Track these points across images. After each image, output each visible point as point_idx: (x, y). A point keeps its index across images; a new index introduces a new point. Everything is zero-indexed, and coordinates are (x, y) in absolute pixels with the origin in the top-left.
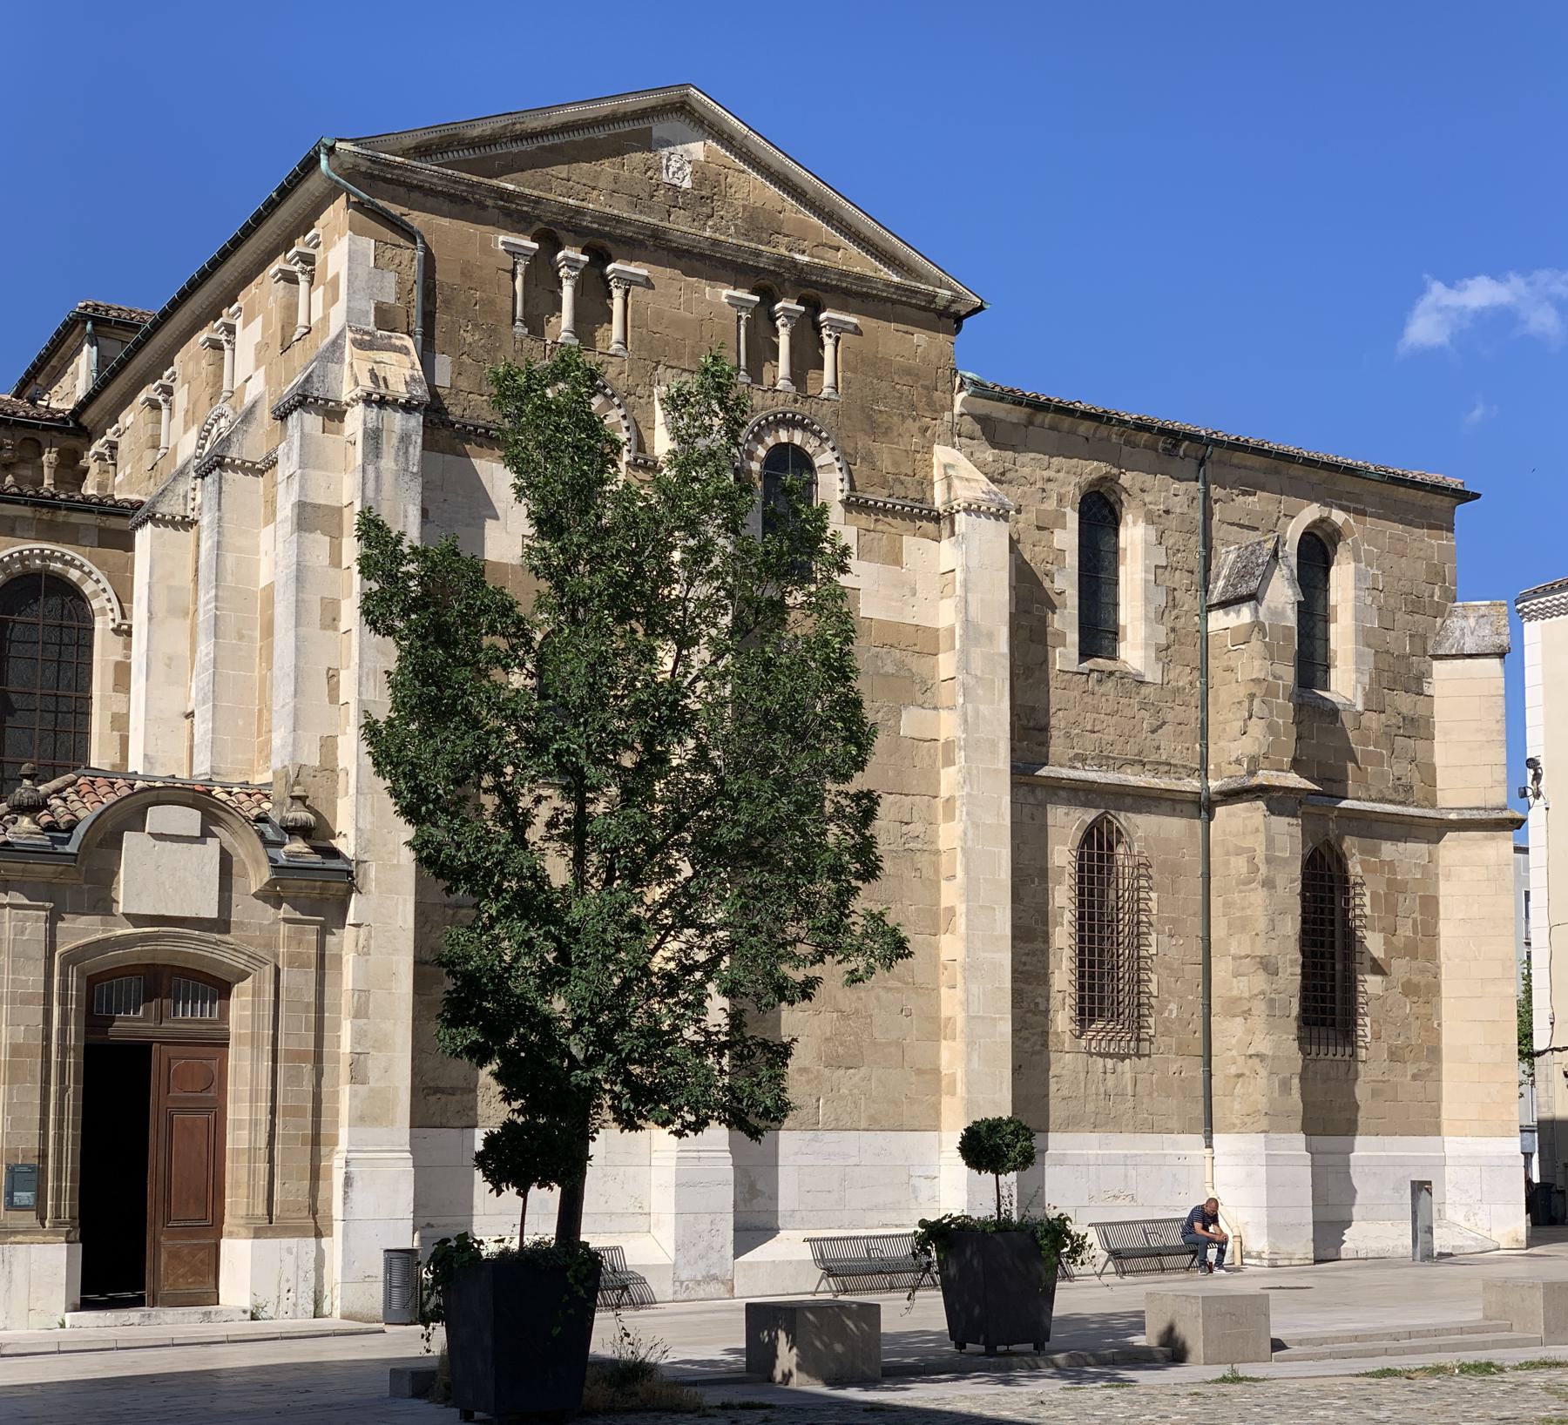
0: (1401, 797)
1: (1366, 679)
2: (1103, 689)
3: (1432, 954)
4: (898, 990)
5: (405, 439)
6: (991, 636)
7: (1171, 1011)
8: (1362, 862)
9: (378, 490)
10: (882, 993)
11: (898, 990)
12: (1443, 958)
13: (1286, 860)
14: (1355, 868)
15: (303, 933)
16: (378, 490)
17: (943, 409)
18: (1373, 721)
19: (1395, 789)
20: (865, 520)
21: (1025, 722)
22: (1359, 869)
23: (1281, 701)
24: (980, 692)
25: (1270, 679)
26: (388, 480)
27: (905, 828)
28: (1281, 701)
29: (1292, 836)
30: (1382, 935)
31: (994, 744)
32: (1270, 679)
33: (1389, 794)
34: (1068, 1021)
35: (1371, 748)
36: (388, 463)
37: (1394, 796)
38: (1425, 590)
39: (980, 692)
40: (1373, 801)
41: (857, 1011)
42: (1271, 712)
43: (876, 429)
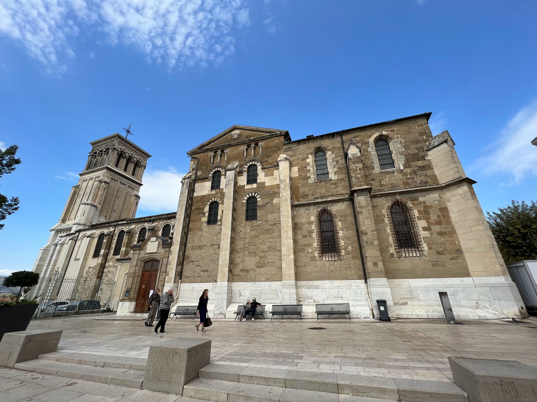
0: (424, 185)
1: (403, 162)
2: (321, 184)
3: (449, 222)
4: (273, 251)
5: (187, 182)
6: (285, 181)
7: (349, 249)
8: (412, 204)
9: (183, 190)
10: (270, 252)
11: (273, 251)
12: (454, 223)
13: (366, 206)
14: (410, 204)
15: (166, 253)
16: (183, 190)
17: (281, 149)
18: (408, 170)
19: (421, 183)
20: (266, 170)
21: (302, 195)
22: (411, 205)
23: (359, 171)
24: (283, 191)
25: (354, 168)
26: (184, 188)
27: (276, 220)
28: (359, 171)
29: (366, 200)
30: (425, 220)
31: (287, 200)
32: (354, 168)
33: (418, 185)
34: (317, 254)
35: (409, 176)
36: (185, 186)
37: (421, 185)
38: (421, 138)
39: (283, 191)
40: (412, 188)
41: (264, 256)
42: (356, 175)
43: (268, 157)
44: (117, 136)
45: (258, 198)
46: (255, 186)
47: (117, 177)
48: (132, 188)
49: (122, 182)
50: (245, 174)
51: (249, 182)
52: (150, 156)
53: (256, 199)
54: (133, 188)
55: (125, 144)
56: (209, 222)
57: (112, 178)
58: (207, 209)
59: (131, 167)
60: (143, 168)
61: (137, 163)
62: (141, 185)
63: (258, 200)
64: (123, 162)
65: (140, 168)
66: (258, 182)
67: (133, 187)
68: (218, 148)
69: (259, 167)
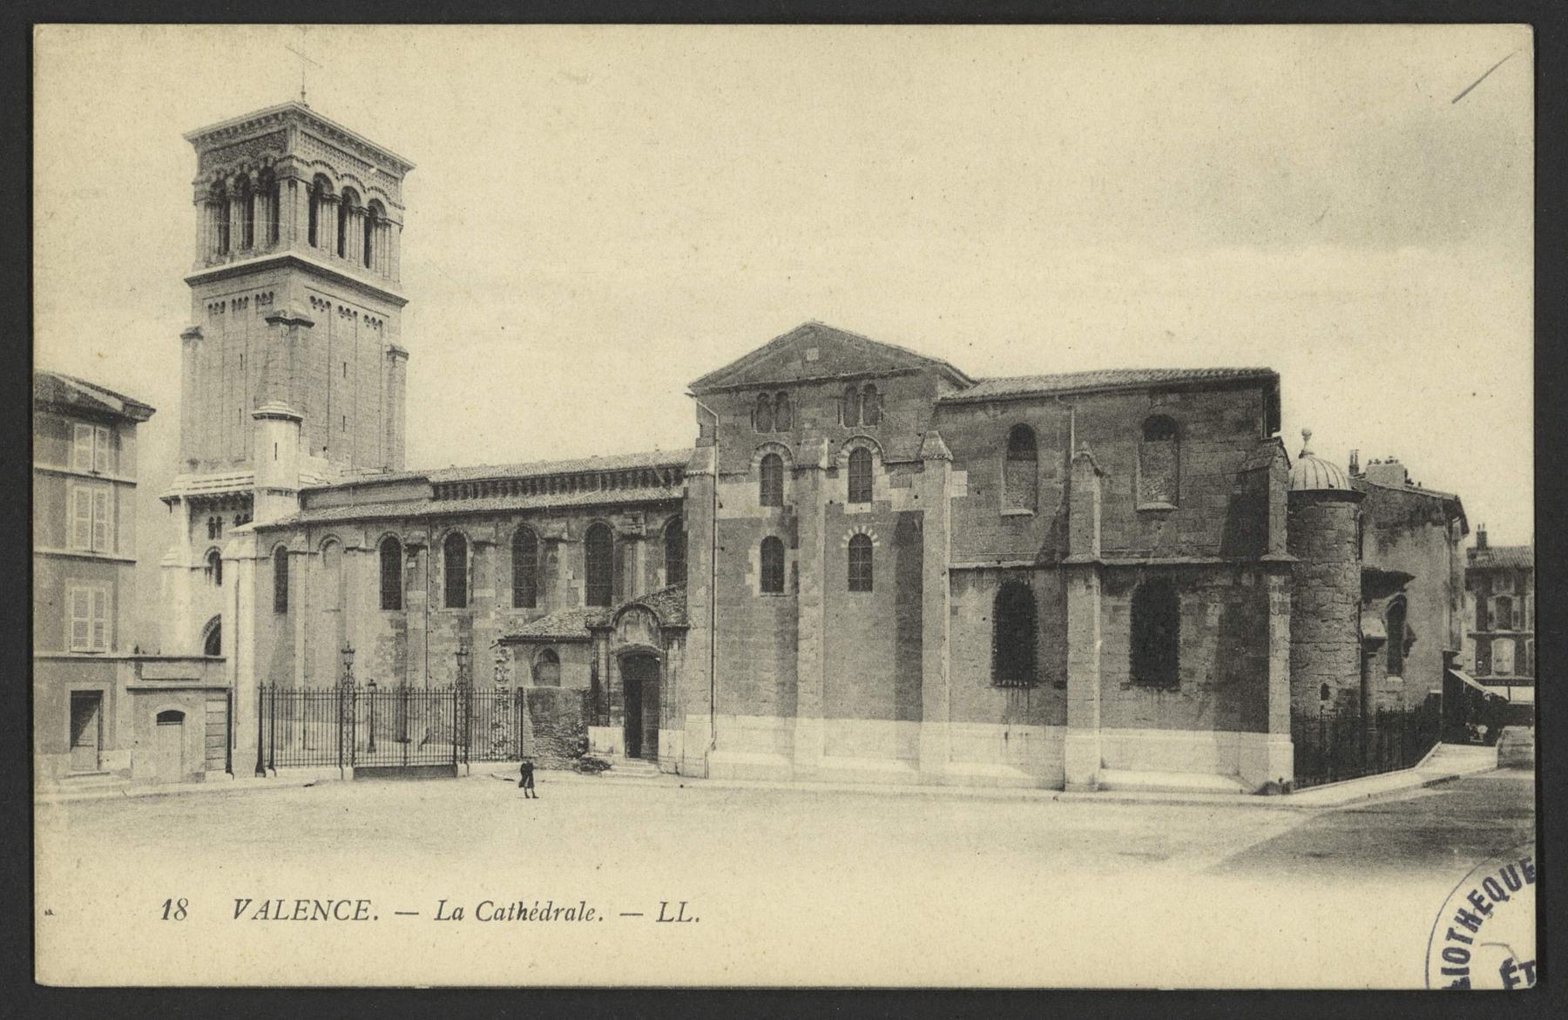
44: (294, 112)
45: (875, 541)
46: (866, 507)
47: (325, 290)
48: (377, 320)
49: (345, 306)
50: (844, 473)
51: (853, 498)
52: (409, 168)
53: (871, 543)
54: (380, 322)
55: (320, 137)
56: (765, 587)
57: (313, 299)
58: (755, 555)
59: (355, 227)
60: (395, 228)
61: (372, 210)
62: (401, 303)
63: (874, 544)
64: (328, 216)
65: (387, 229)
66: (875, 498)
67: (378, 318)
68: (773, 386)
69: (876, 462)
